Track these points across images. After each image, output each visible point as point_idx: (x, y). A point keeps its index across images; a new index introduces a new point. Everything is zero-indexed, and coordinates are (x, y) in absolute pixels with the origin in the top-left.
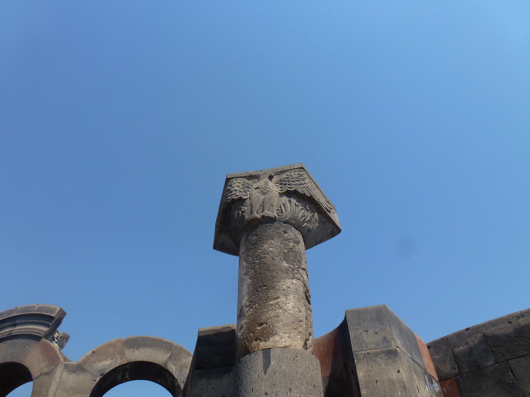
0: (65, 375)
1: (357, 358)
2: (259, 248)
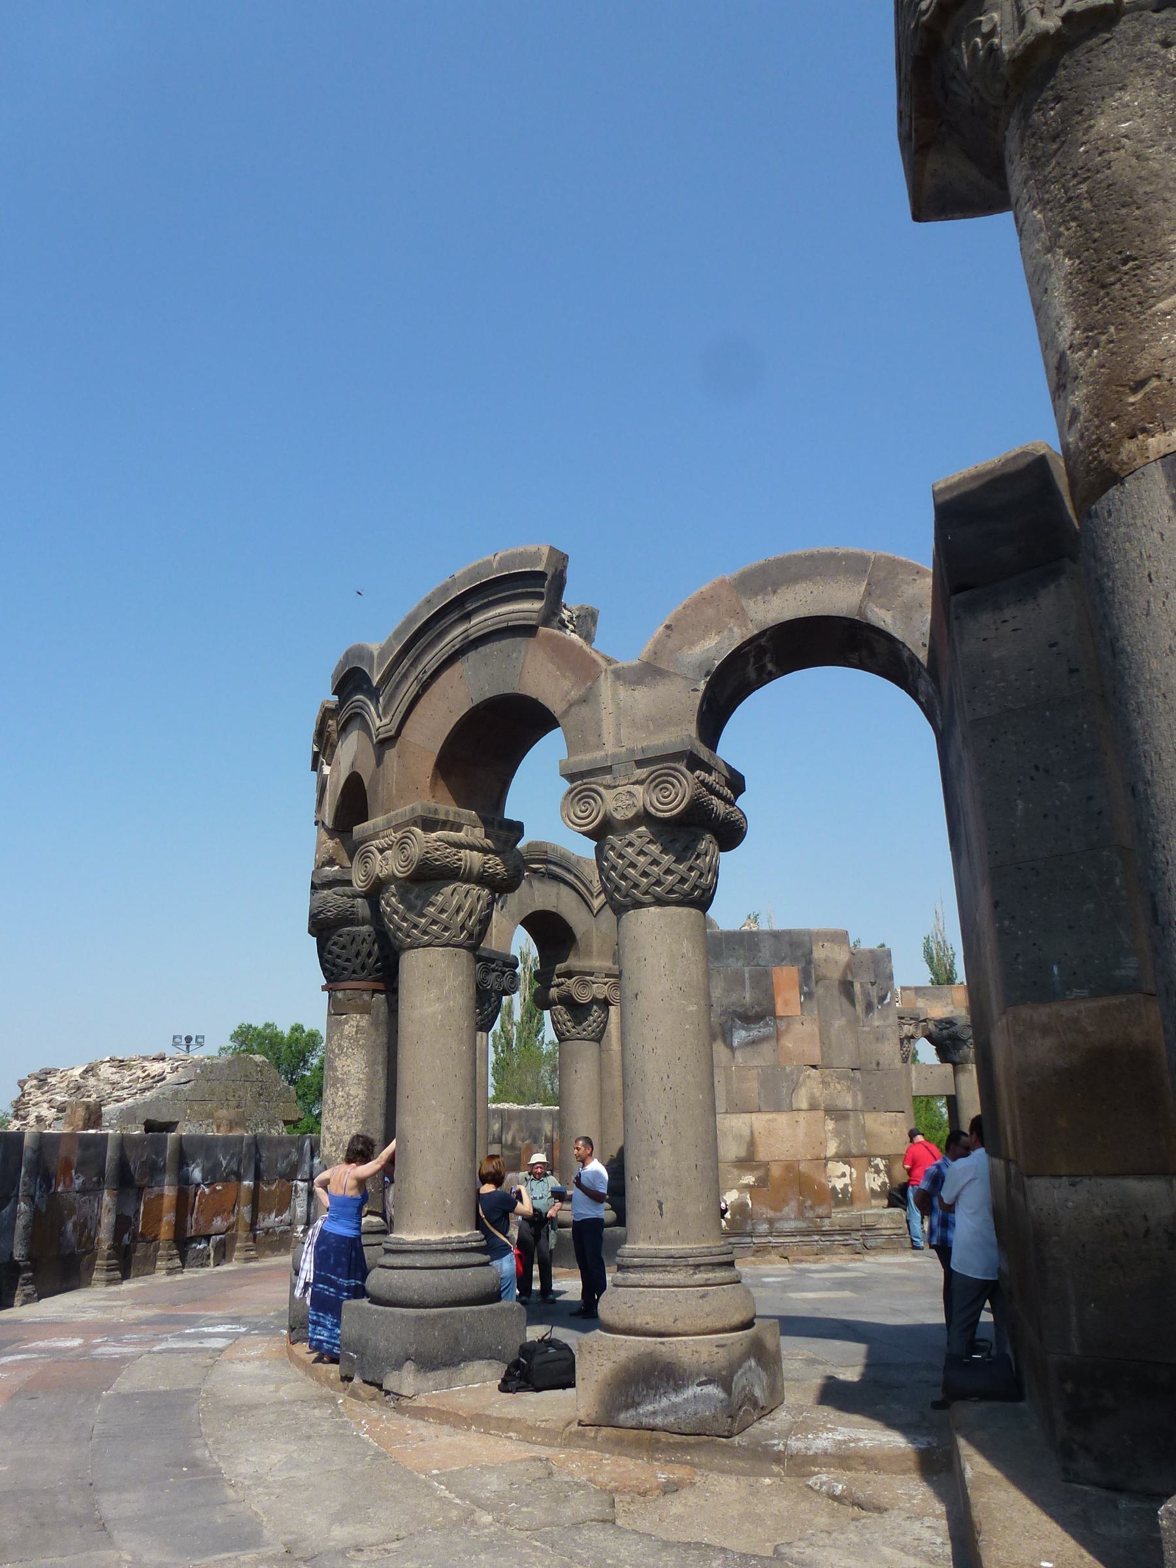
0: (623, 692)
2: (1078, 140)
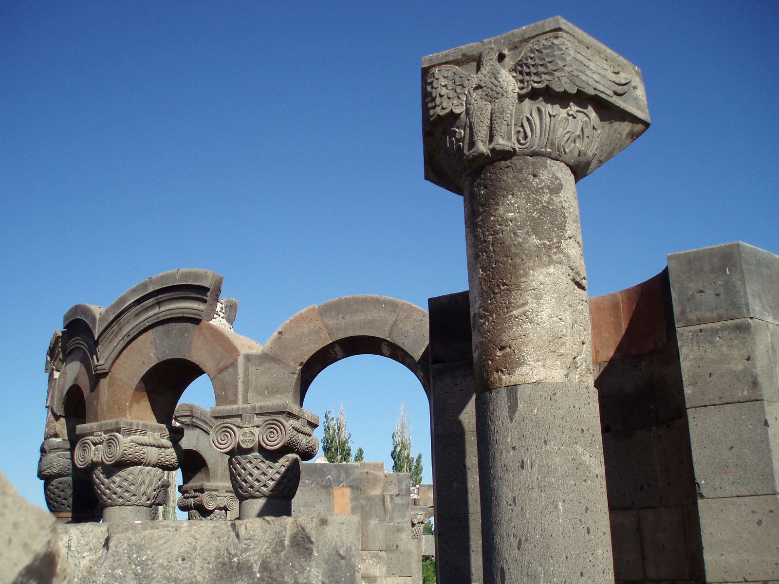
1: (683, 338)
